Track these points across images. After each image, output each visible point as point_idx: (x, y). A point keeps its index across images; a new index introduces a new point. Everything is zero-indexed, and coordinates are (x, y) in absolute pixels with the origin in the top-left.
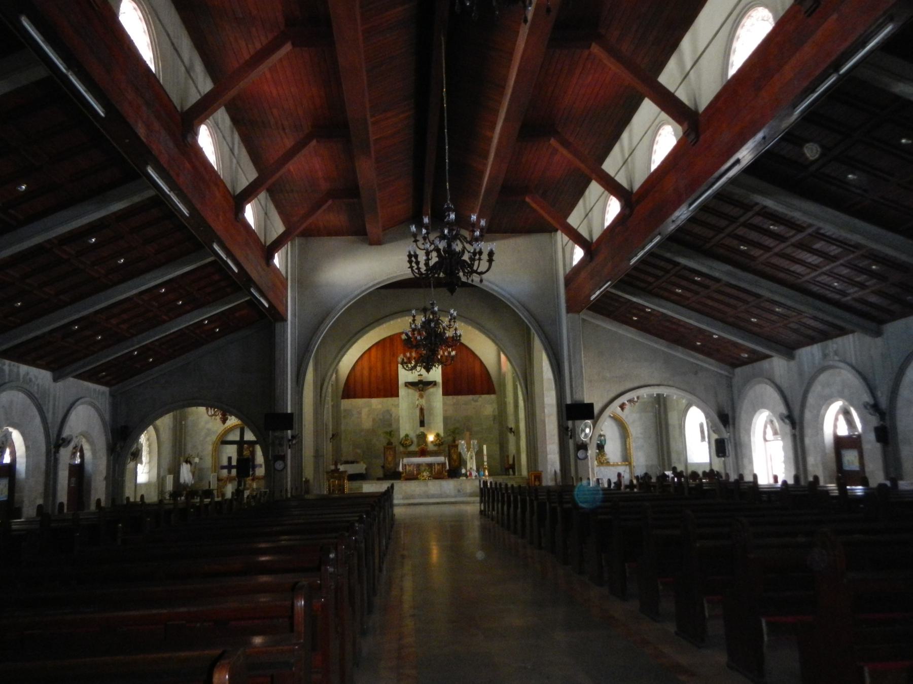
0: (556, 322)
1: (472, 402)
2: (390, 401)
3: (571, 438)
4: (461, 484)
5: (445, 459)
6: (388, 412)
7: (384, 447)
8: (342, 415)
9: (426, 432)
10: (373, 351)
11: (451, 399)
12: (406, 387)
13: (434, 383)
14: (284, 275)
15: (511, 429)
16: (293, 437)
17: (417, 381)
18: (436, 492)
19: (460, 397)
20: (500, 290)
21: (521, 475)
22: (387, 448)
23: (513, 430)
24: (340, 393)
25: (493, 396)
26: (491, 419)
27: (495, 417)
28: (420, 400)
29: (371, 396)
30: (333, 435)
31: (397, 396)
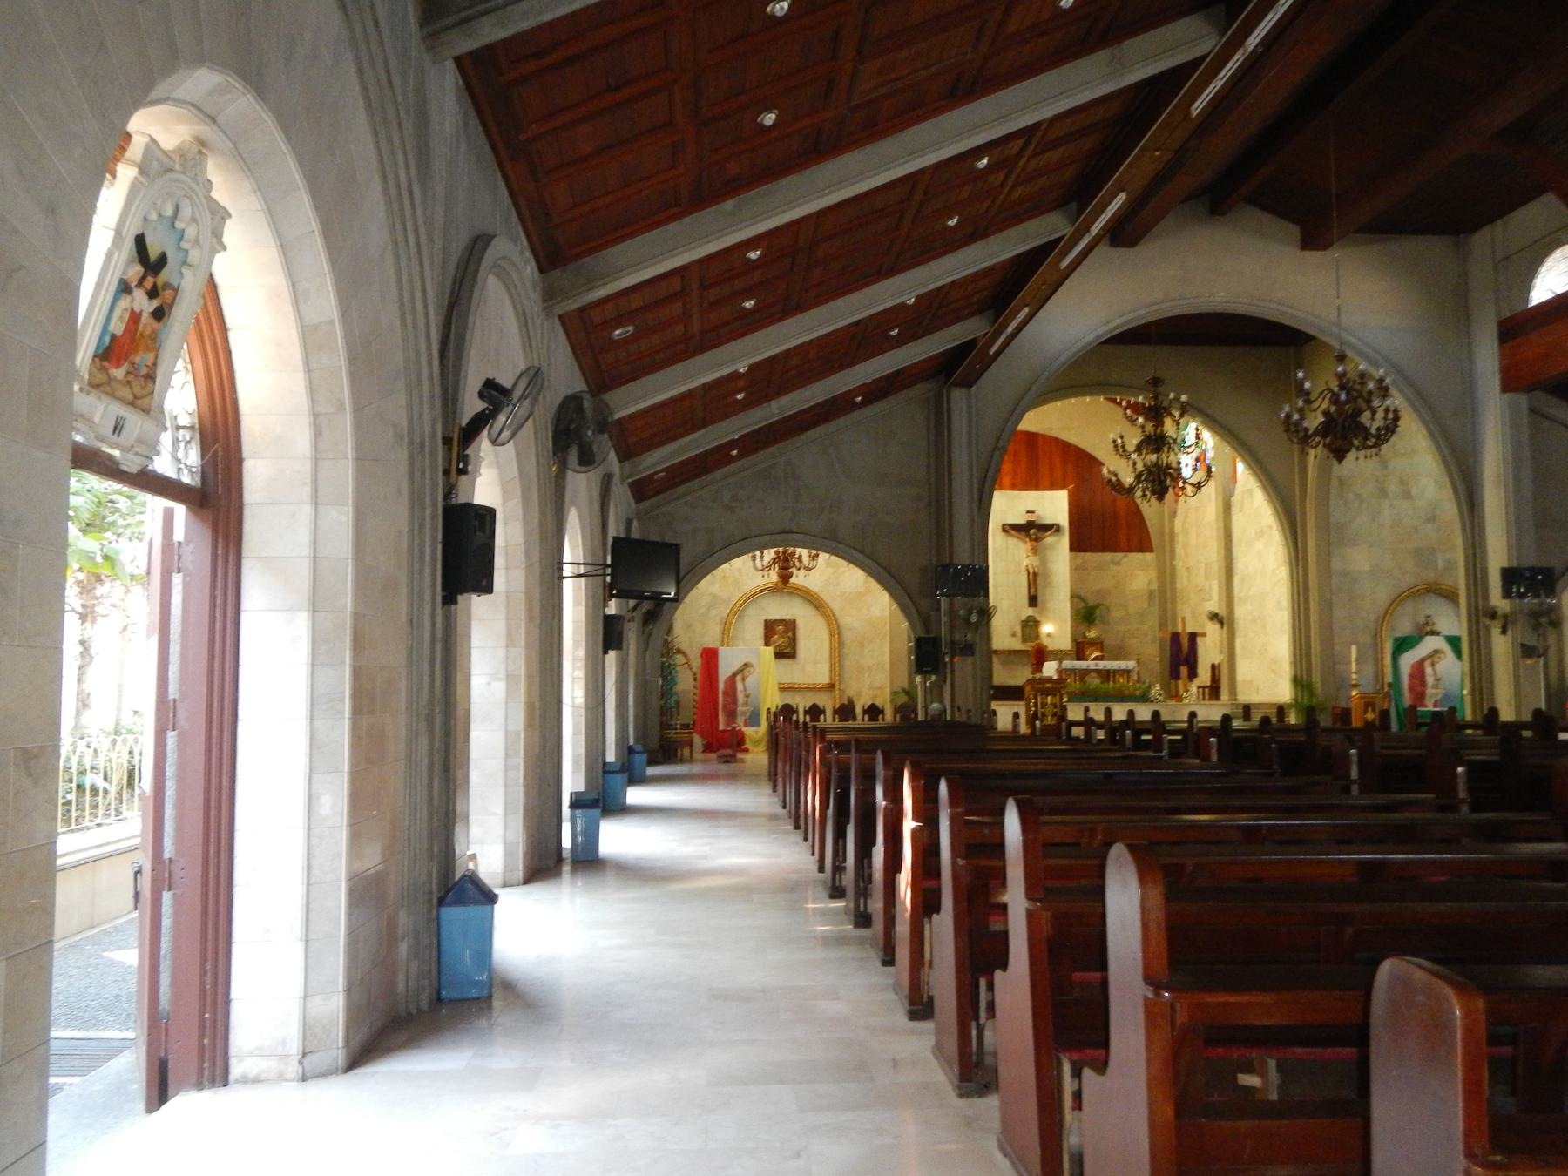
0: (1469, 409)
1: (1112, 566)
9: (1038, 619)
13: (1054, 528)
19: (1088, 555)
21: (1236, 699)
25: (1149, 556)
26: (1145, 597)
27: (1151, 593)
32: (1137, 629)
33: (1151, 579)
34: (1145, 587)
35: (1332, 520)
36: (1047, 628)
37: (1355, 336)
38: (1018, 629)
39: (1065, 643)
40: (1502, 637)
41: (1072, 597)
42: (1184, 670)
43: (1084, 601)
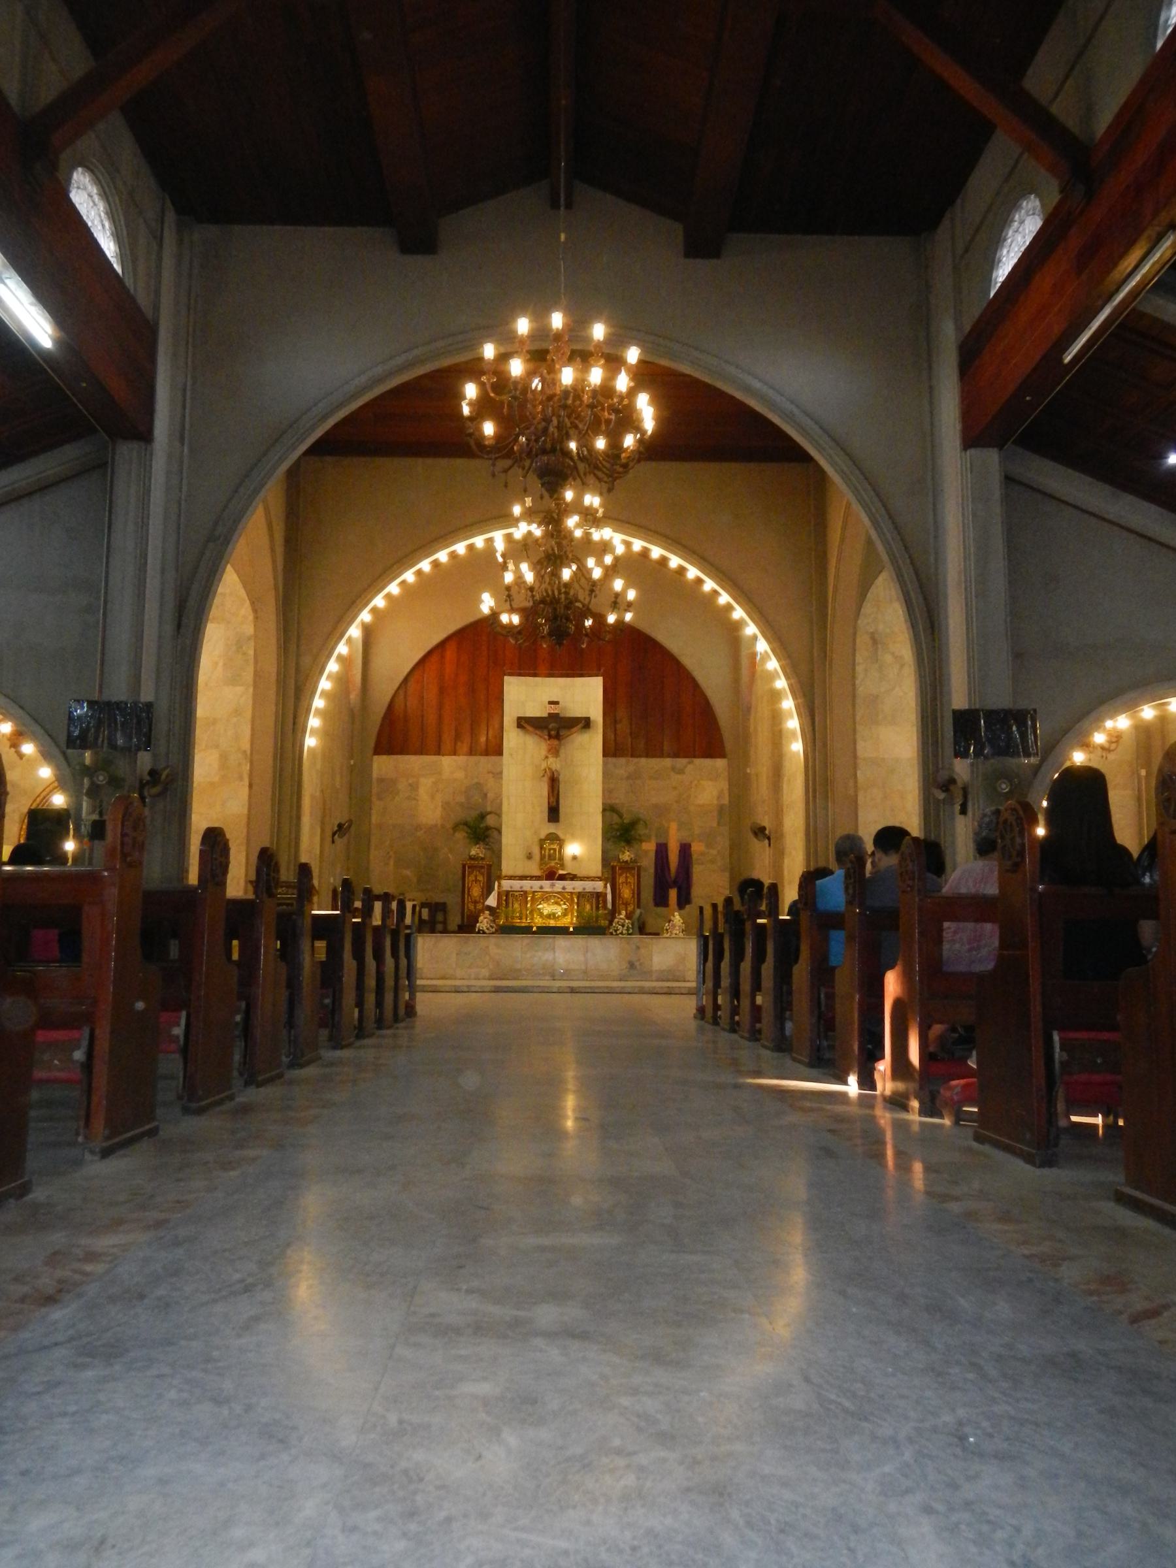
1: (672, 773)
2: (485, 763)
3: (963, 811)
4: (638, 948)
5: (605, 887)
6: (479, 786)
7: (464, 866)
8: (375, 790)
9: (561, 836)
10: (450, 653)
11: (623, 765)
12: (519, 730)
13: (586, 723)
14: (143, 300)
15: (764, 829)
16: (153, 773)
17: (545, 715)
18: (572, 966)
19: (643, 761)
20: (765, 389)
22: (469, 867)
23: (767, 832)
24: (372, 743)
25: (720, 763)
27: (721, 809)
28: (551, 760)
29: (438, 752)
30: (340, 826)
31: (499, 752)
32: (702, 854)
33: (723, 790)
34: (715, 802)
35: (861, 690)
36: (573, 849)
37: (760, 380)
38: (536, 851)
39: (596, 868)
40: (962, 816)
41: (604, 810)
42: (673, 894)
43: (621, 816)
